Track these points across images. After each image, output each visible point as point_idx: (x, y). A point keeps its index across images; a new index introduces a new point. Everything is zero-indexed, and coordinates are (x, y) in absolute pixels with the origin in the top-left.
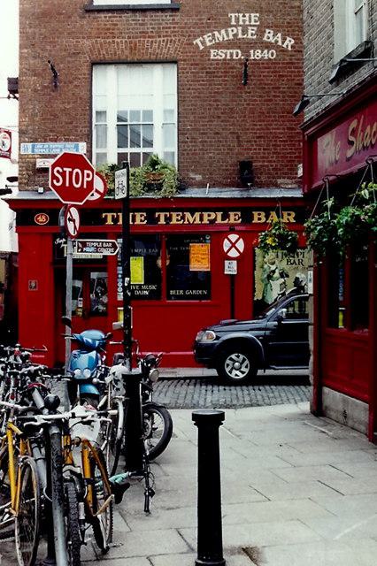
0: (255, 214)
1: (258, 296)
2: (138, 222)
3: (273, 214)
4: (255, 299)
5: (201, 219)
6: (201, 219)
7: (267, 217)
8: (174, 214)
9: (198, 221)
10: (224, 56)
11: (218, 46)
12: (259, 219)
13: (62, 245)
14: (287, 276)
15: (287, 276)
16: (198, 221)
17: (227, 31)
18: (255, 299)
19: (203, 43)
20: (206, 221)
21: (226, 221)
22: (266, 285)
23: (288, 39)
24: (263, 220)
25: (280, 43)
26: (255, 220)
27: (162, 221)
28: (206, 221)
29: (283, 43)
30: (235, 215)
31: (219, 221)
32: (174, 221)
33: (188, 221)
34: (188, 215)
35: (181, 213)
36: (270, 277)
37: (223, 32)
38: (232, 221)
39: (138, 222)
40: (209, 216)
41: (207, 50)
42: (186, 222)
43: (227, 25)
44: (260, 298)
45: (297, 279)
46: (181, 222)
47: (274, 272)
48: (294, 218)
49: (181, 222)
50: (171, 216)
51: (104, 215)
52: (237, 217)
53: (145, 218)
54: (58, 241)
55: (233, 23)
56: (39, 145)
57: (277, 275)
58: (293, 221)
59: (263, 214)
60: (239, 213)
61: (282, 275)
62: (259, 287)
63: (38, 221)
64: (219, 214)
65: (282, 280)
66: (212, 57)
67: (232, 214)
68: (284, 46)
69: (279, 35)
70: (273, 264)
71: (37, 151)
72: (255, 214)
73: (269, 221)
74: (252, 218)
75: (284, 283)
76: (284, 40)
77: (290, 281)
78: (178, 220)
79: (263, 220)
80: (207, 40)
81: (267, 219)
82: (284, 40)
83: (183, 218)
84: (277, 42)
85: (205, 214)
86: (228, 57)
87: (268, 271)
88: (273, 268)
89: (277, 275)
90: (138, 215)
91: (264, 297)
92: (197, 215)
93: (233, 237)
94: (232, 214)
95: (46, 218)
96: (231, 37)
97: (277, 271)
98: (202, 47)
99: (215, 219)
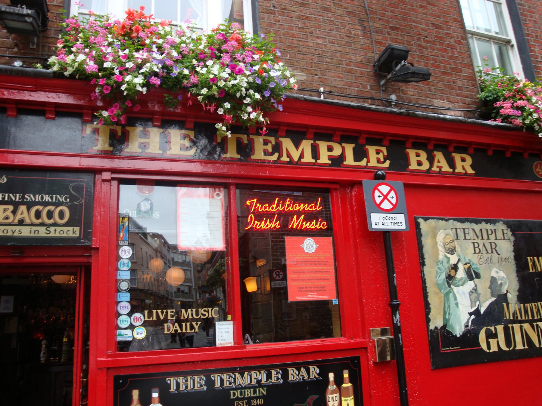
0: (412, 153)
3: (439, 156)
4: (432, 327)
5: (315, 154)
6: (315, 154)
9: (308, 158)
12: (420, 164)
14: (478, 276)
15: (478, 276)
16: (308, 158)
18: (432, 327)
20: (324, 159)
21: (363, 163)
22: (447, 295)
24: (426, 166)
26: (413, 166)
28: (324, 159)
30: (378, 152)
31: (350, 160)
32: (259, 155)
33: (289, 155)
34: (287, 144)
35: (272, 139)
36: (450, 278)
38: (373, 163)
42: (285, 158)
45: (493, 280)
46: (275, 157)
47: (455, 267)
48: (472, 166)
50: (251, 142)
52: (381, 156)
57: (461, 274)
58: (470, 171)
59: (423, 156)
60: (384, 149)
62: (434, 300)
65: (470, 285)
67: (372, 150)
70: (452, 251)
72: (412, 153)
73: (435, 169)
74: (407, 162)
75: (475, 290)
77: (483, 285)
78: (266, 153)
79: (426, 166)
81: (431, 165)
83: (277, 148)
85: (323, 146)
87: (446, 265)
88: (454, 259)
89: (461, 274)
92: (306, 145)
93: (384, 189)
94: (372, 150)
97: (461, 266)
99: (342, 157)
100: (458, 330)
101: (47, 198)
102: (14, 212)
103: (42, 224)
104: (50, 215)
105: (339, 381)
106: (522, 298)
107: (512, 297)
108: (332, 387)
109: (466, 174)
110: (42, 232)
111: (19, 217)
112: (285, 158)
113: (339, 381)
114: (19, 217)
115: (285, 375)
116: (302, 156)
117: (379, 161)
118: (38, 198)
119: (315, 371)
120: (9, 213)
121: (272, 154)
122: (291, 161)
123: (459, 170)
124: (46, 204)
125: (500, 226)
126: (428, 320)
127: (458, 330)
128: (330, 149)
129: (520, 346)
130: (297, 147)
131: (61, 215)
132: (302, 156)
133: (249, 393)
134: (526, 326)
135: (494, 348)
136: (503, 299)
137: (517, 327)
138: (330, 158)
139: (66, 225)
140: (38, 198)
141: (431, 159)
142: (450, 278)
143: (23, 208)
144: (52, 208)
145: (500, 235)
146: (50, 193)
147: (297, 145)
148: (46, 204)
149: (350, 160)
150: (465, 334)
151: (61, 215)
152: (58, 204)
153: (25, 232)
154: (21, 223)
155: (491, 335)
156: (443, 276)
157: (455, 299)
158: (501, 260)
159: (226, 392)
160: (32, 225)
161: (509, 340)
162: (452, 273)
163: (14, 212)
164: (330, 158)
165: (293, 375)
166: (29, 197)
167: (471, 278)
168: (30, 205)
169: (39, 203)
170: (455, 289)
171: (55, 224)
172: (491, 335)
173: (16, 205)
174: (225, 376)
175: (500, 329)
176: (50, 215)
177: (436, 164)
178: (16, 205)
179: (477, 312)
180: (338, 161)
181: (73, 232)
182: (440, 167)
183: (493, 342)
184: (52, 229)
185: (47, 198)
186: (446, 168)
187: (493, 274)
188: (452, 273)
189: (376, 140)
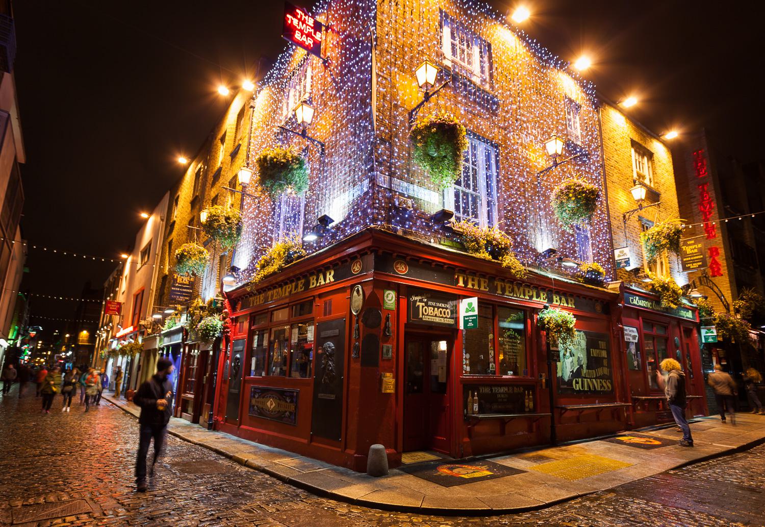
1: (559, 374)
2: (482, 288)
3: (563, 299)
8: (507, 285)
12: (557, 301)
14: (574, 356)
15: (574, 356)
38: (542, 300)
39: (482, 288)
40: (529, 292)
44: (560, 375)
45: (579, 358)
52: (544, 296)
54: (415, 298)
59: (558, 298)
77: (575, 359)
89: (568, 354)
91: (562, 374)
100: (566, 378)
101: (443, 306)
102: (433, 311)
103: (442, 317)
104: (444, 312)
105: (529, 395)
106: (588, 368)
107: (584, 366)
108: (526, 397)
110: (442, 321)
111: (435, 313)
113: (529, 395)
114: (435, 313)
115: (513, 390)
118: (440, 305)
119: (522, 389)
120: (432, 311)
121: (511, 293)
124: (443, 308)
125: (582, 333)
126: (557, 373)
127: (566, 378)
129: (586, 389)
133: (503, 396)
134: (589, 380)
135: (578, 389)
136: (581, 366)
137: (585, 380)
139: (449, 318)
140: (440, 305)
142: (564, 355)
143: (436, 309)
144: (445, 310)
145: (582, 338)
148: (443, 308)
150: (569, 380)
152: (447, 308)
153: (437, 320)
154: (436, 316)
155: (577, 383)
158: (582, 349)
159: (496, 394)
160: (439, 317)
161: (583, 386)
163: (433, 311)
165: (516, 390)
166: (438, 304)
167: (571, 356)
168: (438, 308)
169: (441, 308)
170: (566, 360)
171: (446, 318)
172: (577, 383)
174: (496, 388)
175: (580, 380)
176: (444, 312)
178: (434, 307)
179: (572, 372)
181: (452, 322)
183: (577, 385)
184: (445, 319)
187: (579, 355)
189: (544, 289)
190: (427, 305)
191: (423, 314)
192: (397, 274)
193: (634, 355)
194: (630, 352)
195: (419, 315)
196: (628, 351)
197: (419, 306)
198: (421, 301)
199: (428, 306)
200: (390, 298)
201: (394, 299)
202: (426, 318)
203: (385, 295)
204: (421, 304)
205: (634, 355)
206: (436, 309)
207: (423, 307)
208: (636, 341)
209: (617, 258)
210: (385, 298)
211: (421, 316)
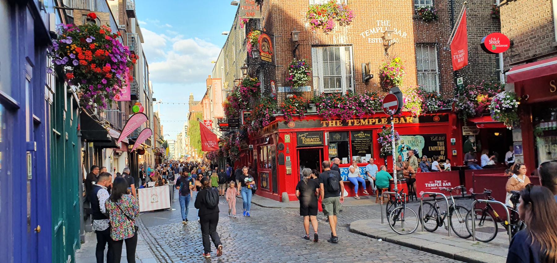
3: (402, 119)
5: (369, 123)
6: (369, 123)
7: (399, 120)
9: (367, 124)
10: (375, 42)
11: (372, 36)
13: (302, 138)
17: (375, 29)
19: (365, 35)
20: (371, 123)
21: (380, 123)
23: (404, 33)
24: (398, 122)
25: (400, 35)
27: (350, 124)
28: (371, 123)
29: (402, 35)
30: (385, 120)
31: (377, 123)
32: (355, 124)
33: (362, 123)
34: (362, 121)
36: (402, 150)
37: (374, 29)
38: (383, 123)
39: (338, 125)
40: (372, 121)
41: (367, 38)
42: (361, 124)
43: (375, 25)
46: (359, 124)
47: (404, 147)
49: (359, 124)
51: (322, 122)
53: (342, 123)
54: (300, 136)
55: (378, 25)
56: (287, 88)
57: (405, 149)
60: (386, 119)
61: (408, 149)
63: (290, 126)
64: (377, 120)
66: (369, 42)
67: (383, 120)
68: (403, 36)
69: (400, 31)
71: (287, 91)
73: (400, 122)
76: (402, 33)
78: (357, 123)
80: (366, 33)
81: (399, 121)
82: (402, 33)
83: (360, 122)
84: (399, 35)
85: (370, 120)
86: (377, 42)
88: (403, 146)
89: (405, 149)
90: (338, 121)
92: (366, 120)
95: (294, 124)
96: (378, 32)
97: (405, 147)
98: (364, 37)
99: (375, 123)
101: (315, 137)
104: (316, 140)
109: (410, 123)
110: (315, 143)
112: (361, 124)
116: (365, 123)
117: (384, 122)
122: (363, 125)
123: (408, 122)
124: (315, 138)
128: (372, 121)
130: (364, 121)
131: (318, 140)
132: (365, 123)
138: (372, 123)
141: (399, 120)
143: (311, 139)
146: (316, 135)
147: (364, 121)
148: (315, 138)
149: (377, 123)
151: (318, 140)
152: (317, 138)
153: (312, 143)
154: (311, 141)
156: (400, 150)
157: (403, 155)
162: (403, 149)
164: (372, 123)
168: (313, 138)
173: (310, 138)
176: (316, 140)
177: (401, 121)
178: (310, 138)
180: (374, 123)
181: (320, 143)
182: (402, 122)
185: (315, 137)
186: (404, 122)
188: (403, 149)
190: (306, 137)
191: (304, 142)
192: (290, 128)
193: (474, 143)
194: (469, 141)
195: (302, 142)
196: (466, 141)
197: (302, 139)
198: (303, 136)
199: (307, 138)
200: (287, 138)
201: (289, 138)
202: (306, 143)
203: (285, 137)
204: (303, 138)
205: (474, 143)
206: (311, 139)
207: (304, 139)
208: (477, 134)
209: (458, 84)
210: (285, 138)
211: (303, 143)
